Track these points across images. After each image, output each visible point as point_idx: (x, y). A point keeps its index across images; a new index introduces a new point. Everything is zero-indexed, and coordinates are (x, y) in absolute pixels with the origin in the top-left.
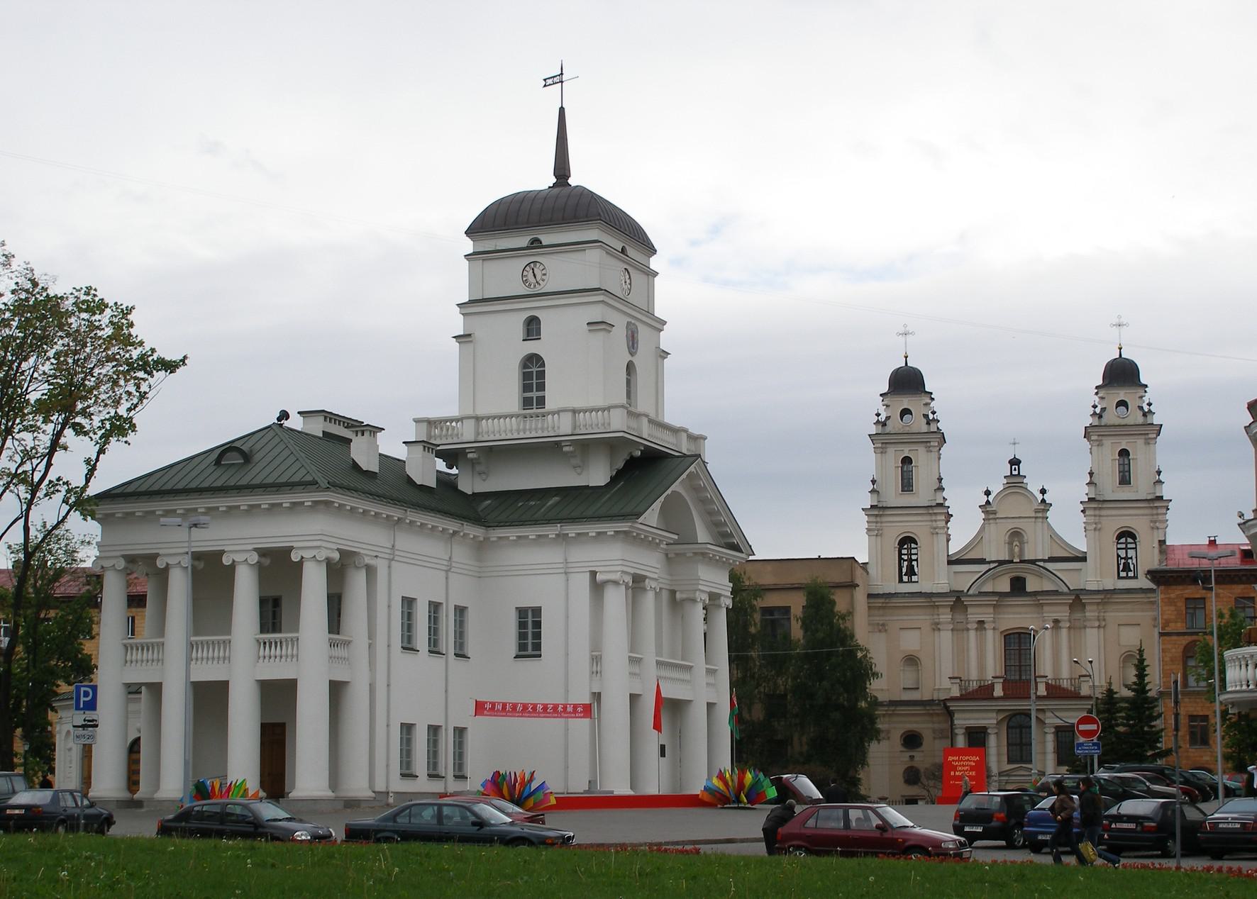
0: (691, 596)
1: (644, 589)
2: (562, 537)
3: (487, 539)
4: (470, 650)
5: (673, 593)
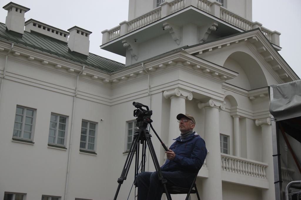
0: (264, 121)
1: (210, 107)
2: (147, 72)
3: (111, 83)
4: (98, 148)
5: (254, 120)
